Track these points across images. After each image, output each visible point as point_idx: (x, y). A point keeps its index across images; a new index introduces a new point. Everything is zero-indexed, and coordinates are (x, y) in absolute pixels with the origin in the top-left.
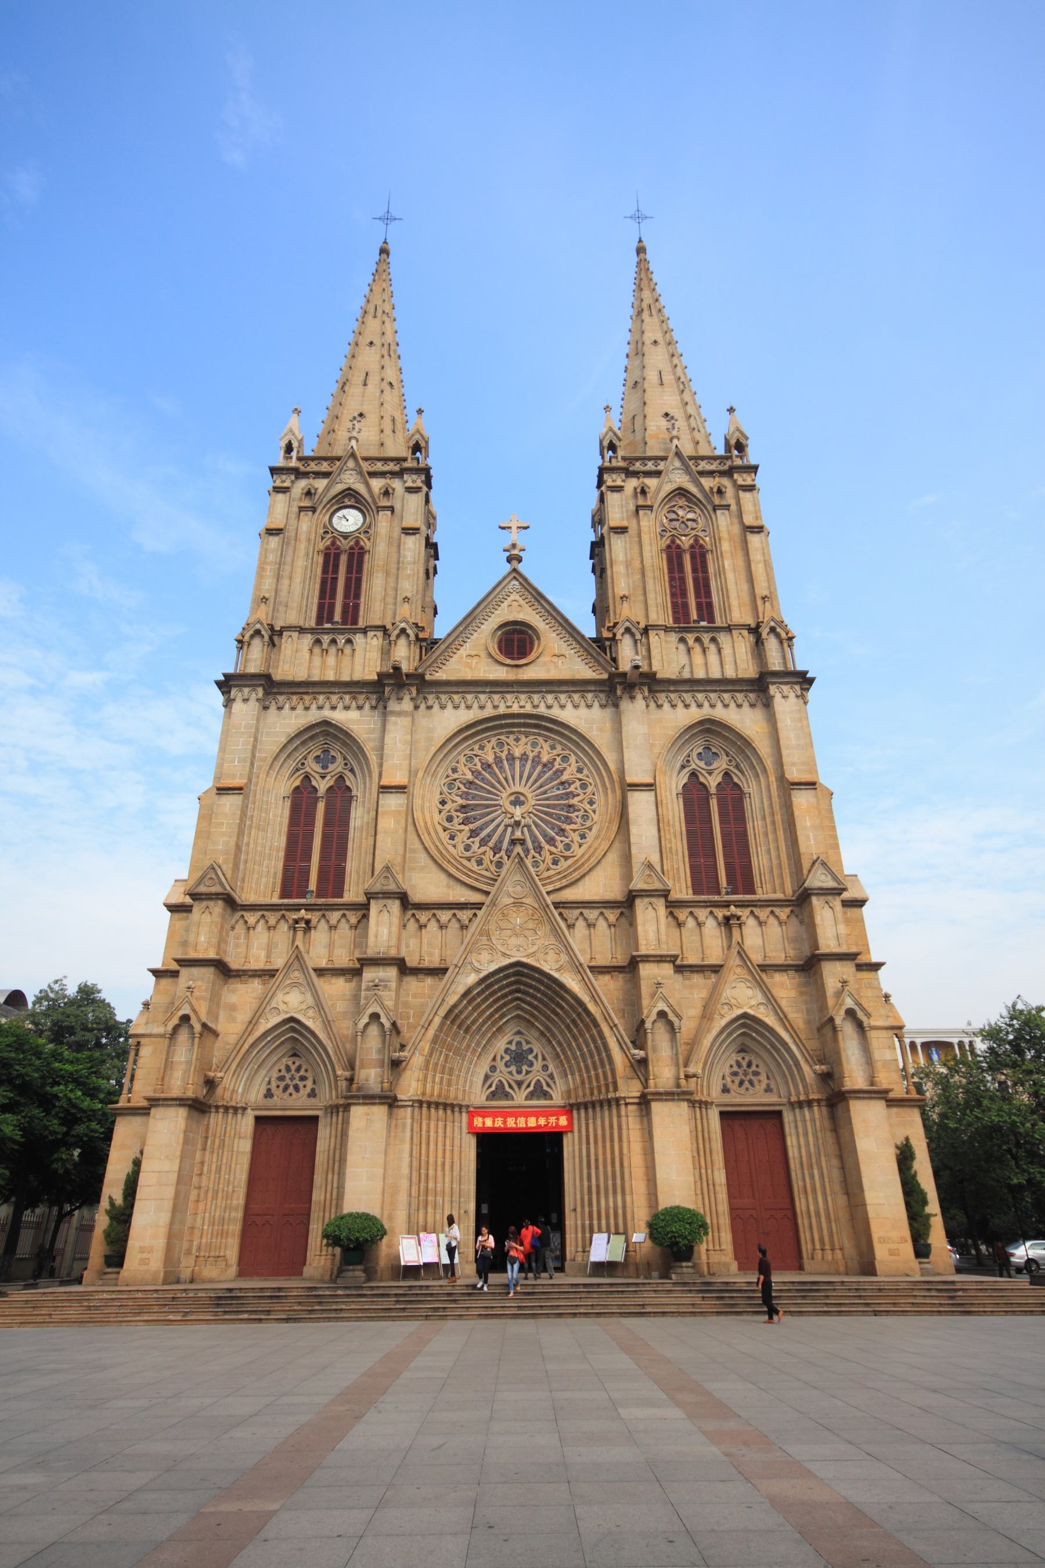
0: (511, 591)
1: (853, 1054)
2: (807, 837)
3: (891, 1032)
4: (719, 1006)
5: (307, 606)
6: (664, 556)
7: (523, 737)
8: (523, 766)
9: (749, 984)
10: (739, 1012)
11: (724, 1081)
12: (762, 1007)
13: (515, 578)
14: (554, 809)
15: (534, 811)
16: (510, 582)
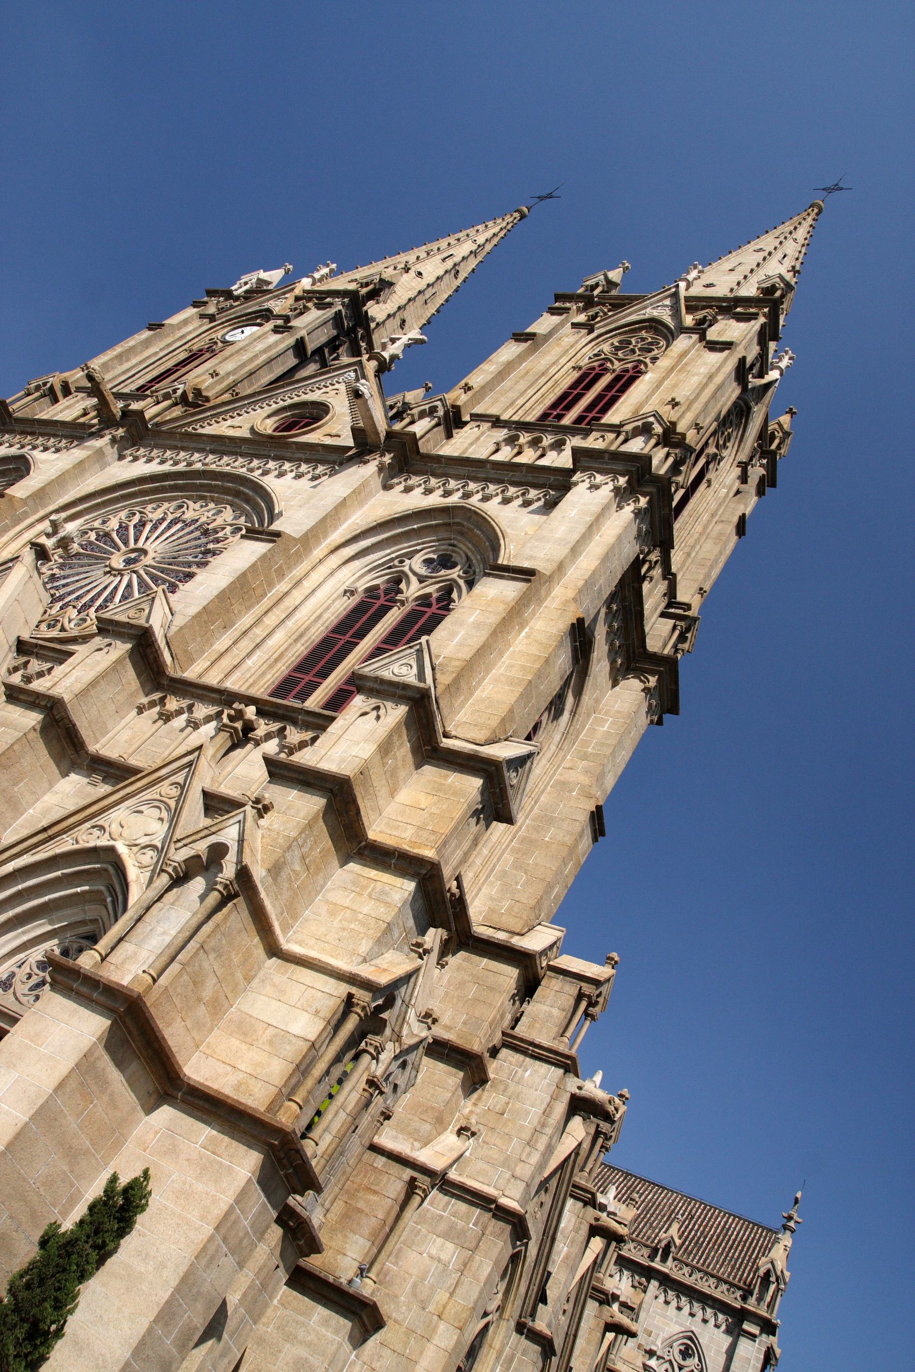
0: (341, 380)
1: (164, 933)
2: (454, 634)
3: (344, 989)
4: (88, 825)
5: (123, 382)
6: (576, 375)
7: (212, 505)
8: (182, 529)
9: (165, 815)
10: (104, 842)
11: (16, 970)
12: (150, 853)
13: (355, 371)
14: (168, 574)
15: (142, 572)
16: (345, 373)
